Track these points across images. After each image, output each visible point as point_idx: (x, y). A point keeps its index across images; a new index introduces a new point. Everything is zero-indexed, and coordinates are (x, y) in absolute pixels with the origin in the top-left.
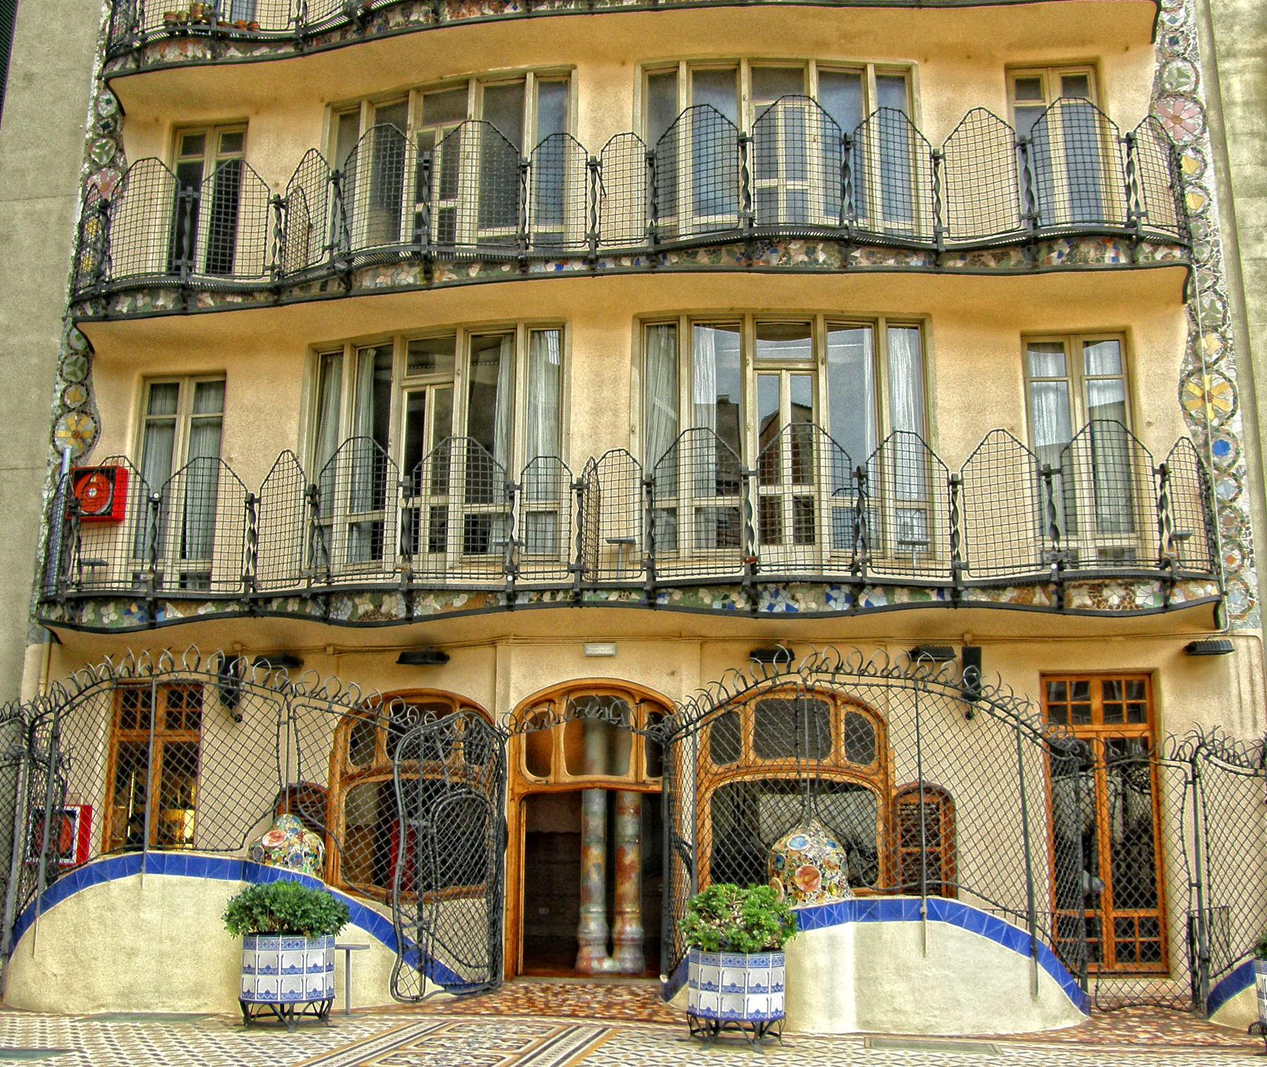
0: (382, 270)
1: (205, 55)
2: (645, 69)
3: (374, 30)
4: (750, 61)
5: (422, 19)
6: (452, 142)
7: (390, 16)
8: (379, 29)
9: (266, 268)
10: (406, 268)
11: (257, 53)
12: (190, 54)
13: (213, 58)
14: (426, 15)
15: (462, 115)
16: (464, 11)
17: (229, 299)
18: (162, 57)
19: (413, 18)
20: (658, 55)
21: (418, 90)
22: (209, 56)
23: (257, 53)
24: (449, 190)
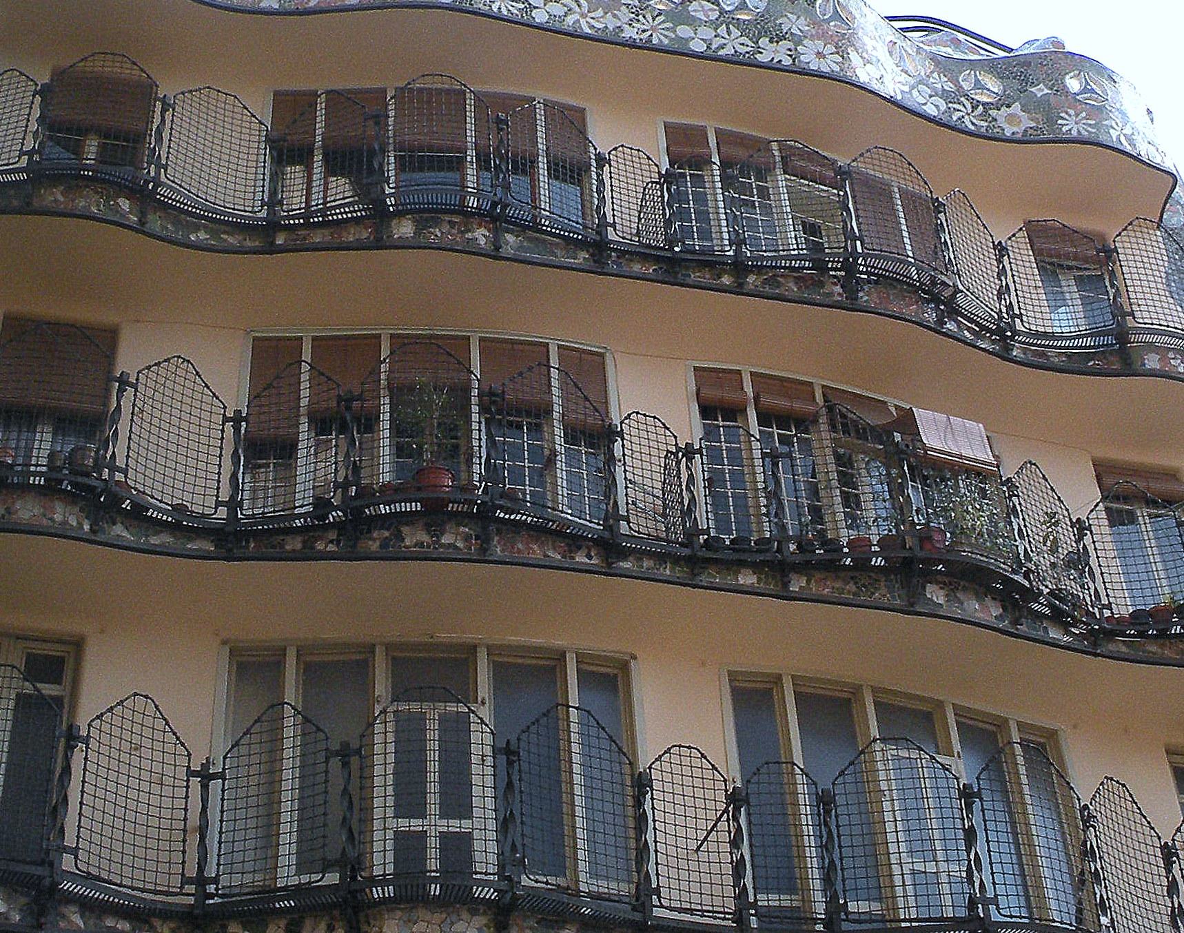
0: (422, 913)
1: (80, 525)
2: (733, 677)
3: (374, 546)
4: (875, 690)
5: (460, 544)
6: (456, 731)
7: (405, 530)
8: (385, 544)
9: (186, 881)
10: (465, 915)
11: (155, 540)
12: (58, 517)
13: (92, 531)
14: (467, 538)
15: (467, 695)
16: (520, 546)
17: (110, 922)
18: (8, 510)
19: (446, 539)
20: (758, 662)
21: (388, 647)
22: (86, 527)
23: (155, 540)
24: (457, 801)
